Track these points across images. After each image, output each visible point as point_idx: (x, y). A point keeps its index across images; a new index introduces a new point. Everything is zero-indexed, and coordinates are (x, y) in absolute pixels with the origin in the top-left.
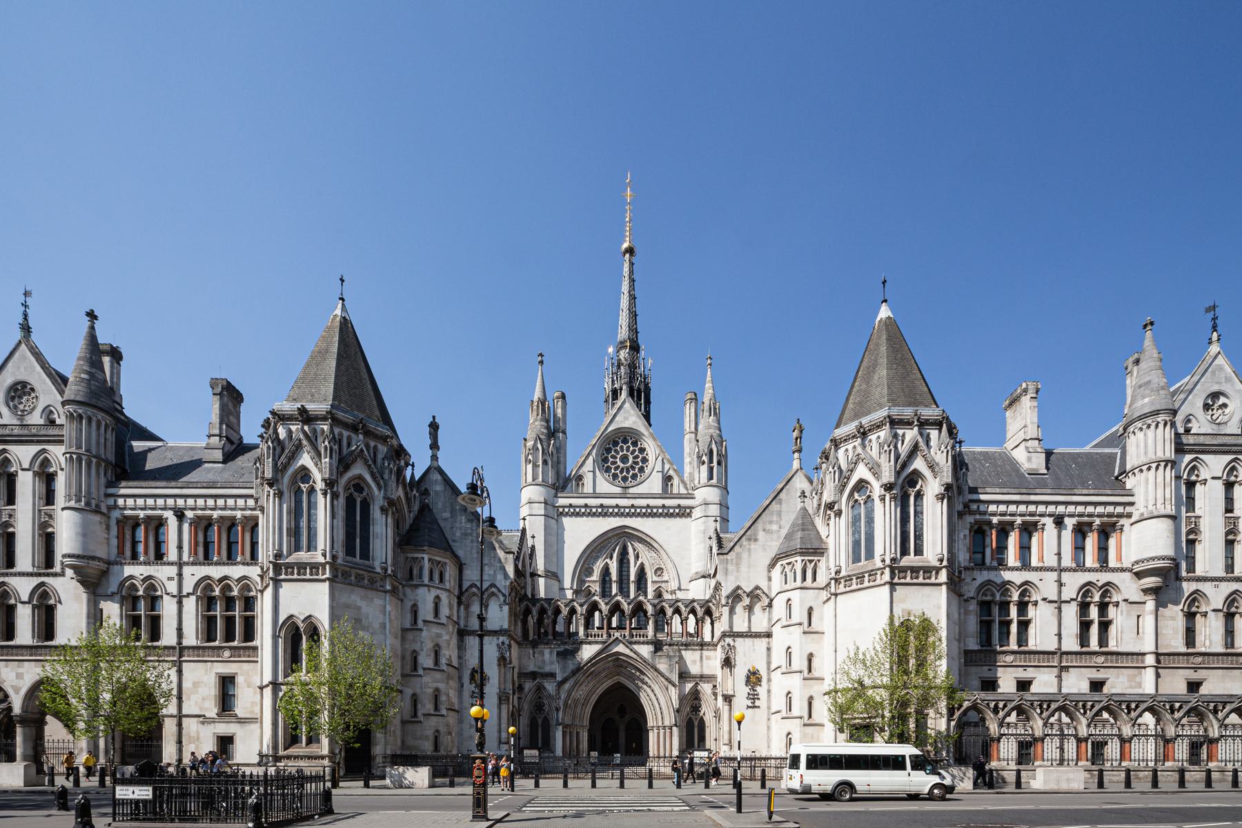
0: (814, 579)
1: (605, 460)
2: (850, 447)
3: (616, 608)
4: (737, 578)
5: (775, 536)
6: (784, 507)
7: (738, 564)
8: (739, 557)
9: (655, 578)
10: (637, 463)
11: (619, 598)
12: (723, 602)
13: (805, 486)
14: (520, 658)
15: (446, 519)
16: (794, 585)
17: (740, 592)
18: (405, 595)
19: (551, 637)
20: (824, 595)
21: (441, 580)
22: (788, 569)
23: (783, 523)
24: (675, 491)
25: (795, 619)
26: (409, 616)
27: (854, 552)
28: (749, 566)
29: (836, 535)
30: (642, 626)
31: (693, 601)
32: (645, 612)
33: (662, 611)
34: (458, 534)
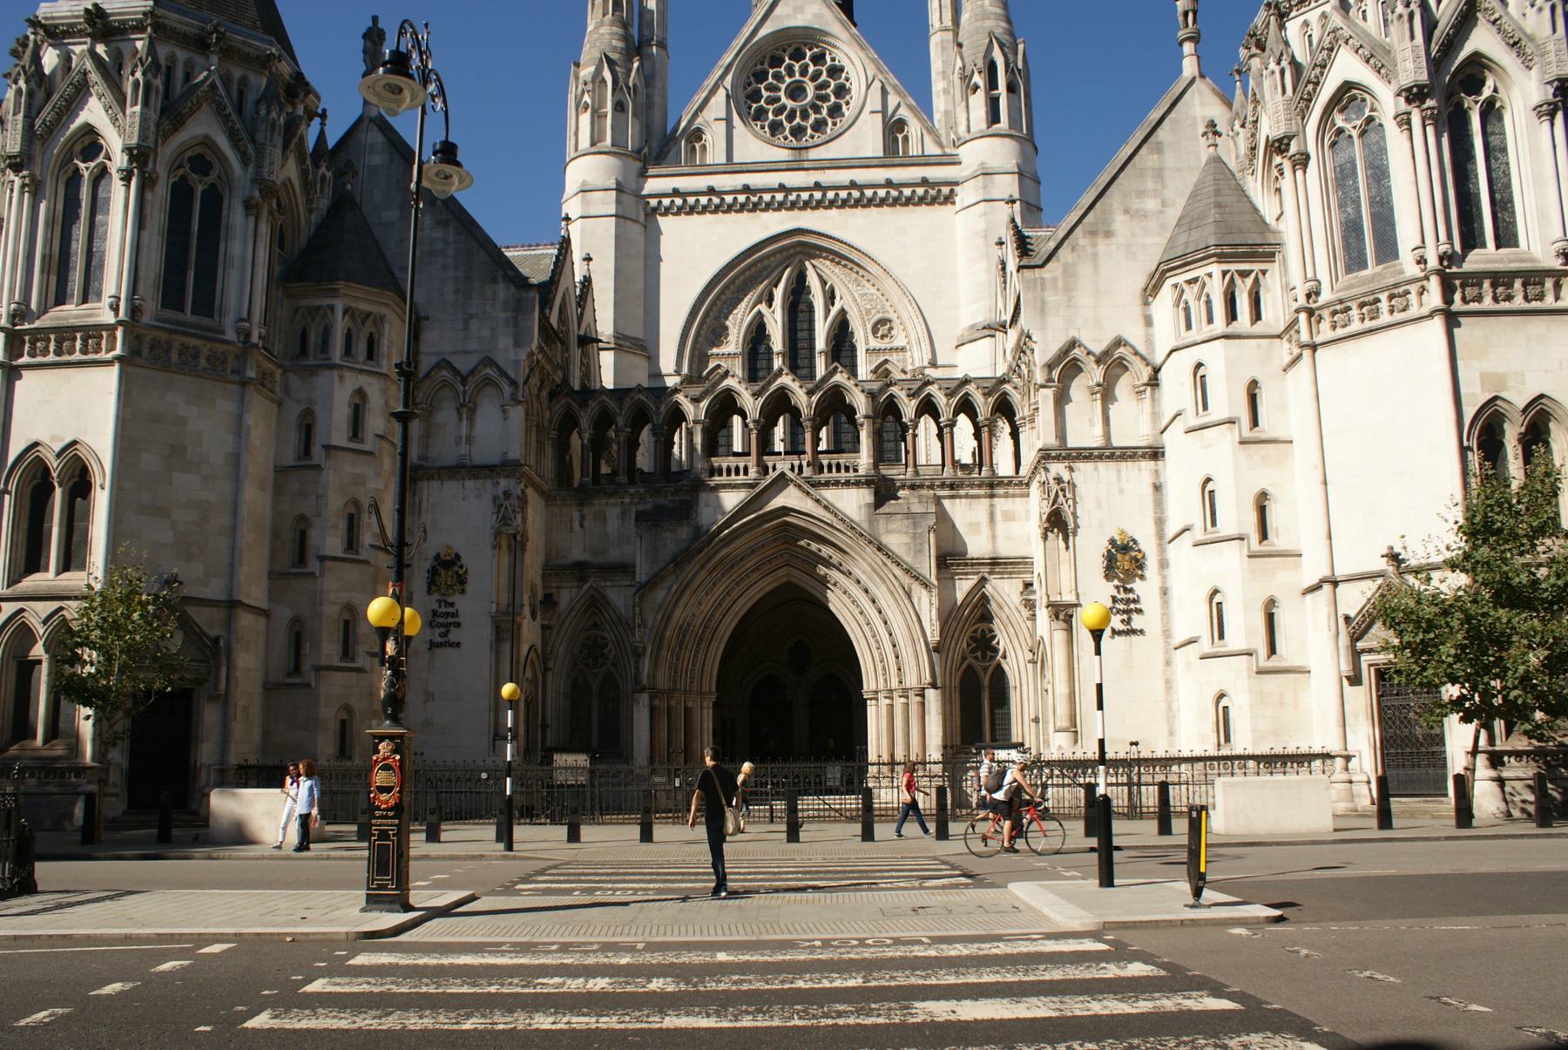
0: (1257, 315)
1: (756, 96)
2: (1313, 16)
3: (779, 404)
6: (1169, 159)
7: (1069, 290)
9: (875, 343)
10: (825, 98)
11: (786, 380)
13: (1217, 111)
14: (548, 532)
16: (1208, 331)
18: (287, 390)
19: (623, 479)
20: (1285, 350)
23: (1169, 194)
25: (1218, 410)
26: (293, 439)
27: (1347, 246)
29: (1299, 212)
30: (844, 443)
31: (966, 381)
32: (851, 411)
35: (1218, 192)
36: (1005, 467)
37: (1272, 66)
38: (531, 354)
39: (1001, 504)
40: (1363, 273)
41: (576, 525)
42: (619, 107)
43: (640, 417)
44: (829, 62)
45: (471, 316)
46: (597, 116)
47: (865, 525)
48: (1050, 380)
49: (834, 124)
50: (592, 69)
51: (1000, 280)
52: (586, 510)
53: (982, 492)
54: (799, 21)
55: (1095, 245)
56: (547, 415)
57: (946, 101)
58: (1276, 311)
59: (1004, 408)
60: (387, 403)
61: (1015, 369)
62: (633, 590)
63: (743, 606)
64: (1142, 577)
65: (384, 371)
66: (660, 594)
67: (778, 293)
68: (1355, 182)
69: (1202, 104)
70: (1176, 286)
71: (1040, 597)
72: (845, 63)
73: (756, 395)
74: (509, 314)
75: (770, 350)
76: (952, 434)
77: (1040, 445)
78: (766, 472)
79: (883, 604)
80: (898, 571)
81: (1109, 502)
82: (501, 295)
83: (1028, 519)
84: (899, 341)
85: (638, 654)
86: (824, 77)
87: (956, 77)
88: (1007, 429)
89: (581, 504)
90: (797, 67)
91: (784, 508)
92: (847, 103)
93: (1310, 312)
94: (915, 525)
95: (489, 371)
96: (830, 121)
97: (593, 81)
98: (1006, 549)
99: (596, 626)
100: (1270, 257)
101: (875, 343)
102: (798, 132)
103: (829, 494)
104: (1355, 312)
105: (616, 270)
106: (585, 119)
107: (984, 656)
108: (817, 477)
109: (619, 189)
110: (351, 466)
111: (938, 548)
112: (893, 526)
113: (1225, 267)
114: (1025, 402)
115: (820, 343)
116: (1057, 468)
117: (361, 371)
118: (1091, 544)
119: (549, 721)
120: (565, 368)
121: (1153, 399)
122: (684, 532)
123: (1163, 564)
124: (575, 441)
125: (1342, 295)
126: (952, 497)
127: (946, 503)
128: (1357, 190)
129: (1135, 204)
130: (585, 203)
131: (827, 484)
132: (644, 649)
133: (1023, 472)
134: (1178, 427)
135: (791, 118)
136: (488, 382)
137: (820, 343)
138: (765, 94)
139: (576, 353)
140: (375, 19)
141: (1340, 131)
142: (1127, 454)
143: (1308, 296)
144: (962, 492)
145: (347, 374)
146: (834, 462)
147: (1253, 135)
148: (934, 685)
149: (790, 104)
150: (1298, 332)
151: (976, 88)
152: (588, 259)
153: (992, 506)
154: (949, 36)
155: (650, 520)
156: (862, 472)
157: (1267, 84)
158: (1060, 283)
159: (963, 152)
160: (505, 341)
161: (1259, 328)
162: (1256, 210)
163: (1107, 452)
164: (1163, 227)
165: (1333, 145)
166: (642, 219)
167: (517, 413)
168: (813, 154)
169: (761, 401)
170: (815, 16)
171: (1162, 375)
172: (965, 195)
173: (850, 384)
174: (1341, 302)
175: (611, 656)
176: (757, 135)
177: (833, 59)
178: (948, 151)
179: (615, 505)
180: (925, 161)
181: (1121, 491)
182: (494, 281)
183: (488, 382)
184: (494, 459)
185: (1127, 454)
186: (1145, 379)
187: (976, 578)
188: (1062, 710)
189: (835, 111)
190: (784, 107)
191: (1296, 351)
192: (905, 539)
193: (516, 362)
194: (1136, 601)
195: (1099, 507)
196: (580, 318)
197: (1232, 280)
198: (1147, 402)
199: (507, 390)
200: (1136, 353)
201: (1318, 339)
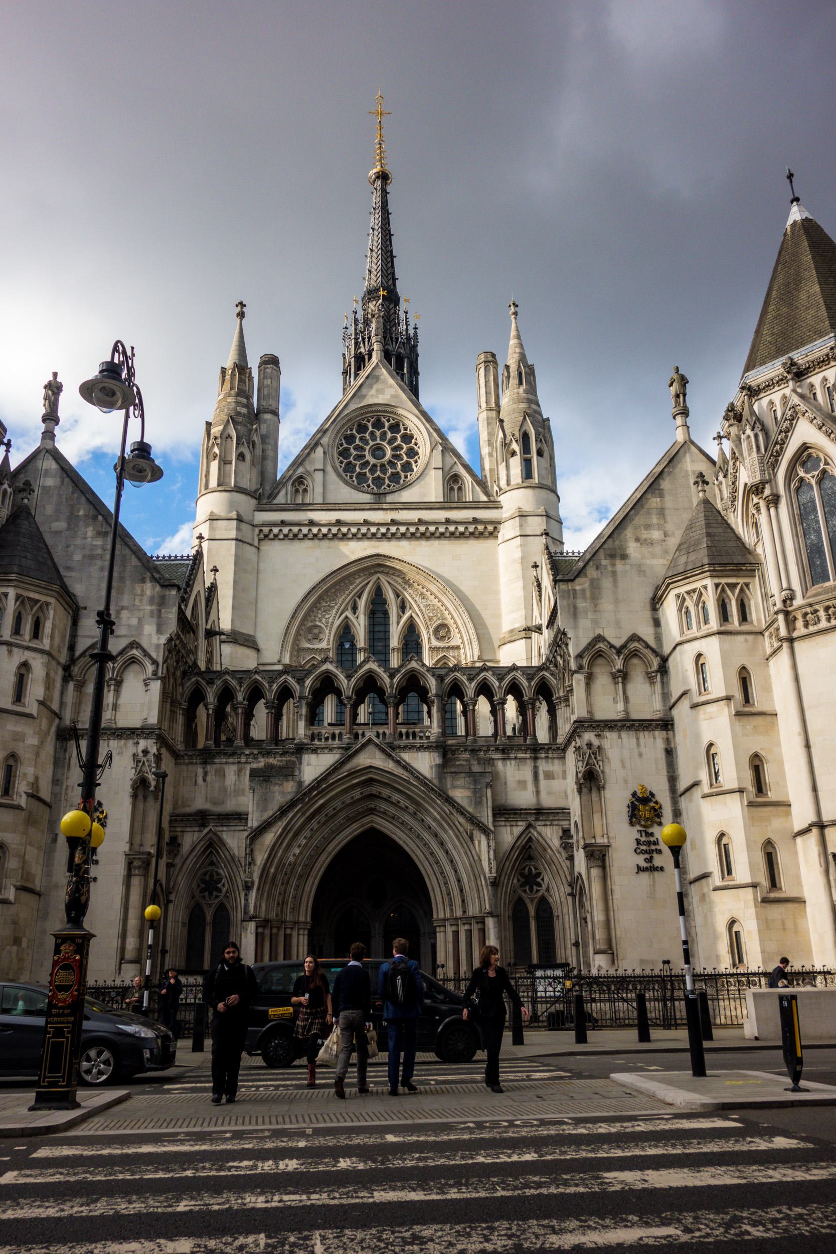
0: (744, 618)
3: (369, 686)
4: (595, 623)
5: (657, 549)
6: (669, 502)
8: (595, 586)
9: (435, 643)
11: (373, 666)
12: (573, 665)
15: (58, 533)
16: (705, 630)
17: (601, 645)
21: (36, 634)
22: (689, 603)
23: (669, 527)
24: (469, 497)
28: (617, 601)
31: (514, 668)
33: (456, 690)
34: (77, 557)
35: (708, 525)
36: (542, 735)
37: (749, 431)
38: (170, 640)
39: (543, 766)
40: (827, 584)
41: (200, 780)
42: (241, 457)
43: (256, 694)
44: (402, 432)
45: (123, 608)
46: (224, 462)
47: (435, 782)
48: (581, 667)
49: (406, 477)
50: (221, 428)
51: (535, 594)
52: (209, 767)
53: (528, 756)
54: (380, 399)
55: (614, 565)
56: (180, 689)
57: (491, 462)
58: (758, 614)
59: (544, 691)
60: (48, 675)
61: (551, 661)
62: (246, 834)
63: (334, 847)
64: (660, 824)
65: (47, 648)
66: (269, 838)
67: (362, 603)
68: (816, 516)
69: (692, 461)
70: (678, 596)
71: (577, 839)
72: (415, 432)
73: (349, 677)
74: (154, 607)
75: (353, 645)
76: (503, 710)
77: (574, 718)
78: (356, 736)
79: (450, 846)
80: (462, 820)
81: (630, 764)
82: (148, 593)
83: (564, 778)
84: (453, 643)
85: (248, 887)
86: (399, 441)
87: (499, 444)
88: (543, 708)
89: (205, 763)
90: (378, 433)
91: (371, 767)
92: (416, 462)
93: (787, 614)
94: (475, 782)
95: (135, 652)
96: (402, 474)
97: (221, 437)
98: (547, 801)
99: (212, 863)
100: (751, 573)
101: (435, 643)
102: (378, 481)
103: (406, 756)
104: (822, 613)
105: (235, 582)
106: (214, 465)
107: (531, 890)
108: (397, 743)
109: (239, 519)
110: (12, 726)
111: (494, 801)
112: (459, 783)
113: (717, 581)
114: (561, 686)
115: (395, 641)
116: (589, 736)
117: (28, 648)
118: (616, 798)
119: (168, 948)
120: (195, 651)
121: (662, 683)
122: (290, 787)
123: (677, 814)
124: (201, 712)
125: (811, 600)
126: (504, 759)
127: (500, 764)
128: (818, 522)
129: (644, 534)
130: (211, 528)
131: (406, 748)
132: (253, 883)
133: (560, 740)
134: (685, 704)
135: (373, 469)
136: (133, 660)
137: (395, 641)
138: (354, 453)
139: (202, 643)
140: (55, 375)
141: (802, 480)
142: (644, 725)
143: (784, 601)
144: (512, 756)
145: (15, 650)
146: (411, 731)
147: (734, 483)
148: (491, 914)
149: (372, 461)
150: (778, 629)
151: (513, 454)
152: (215, 570)
153: (536, 768)
154: (494, 414)
155: (262, 777)
156: (432, 739)
157: (744, 445)
158: (588, 594)
159: (502, 499)
160: (149, 629)
161: (746, 627)
162: (738, 538)
163: (628, 724)
164: (666, 552)
165: (798, 489)
166: (256, 543)
167: (156, 686)
168: (389, 498)
169: (353, 681)
170: (393, 396)
171: (671, 663)
172: (508, 530)
173: (423, 670)
174: (811, 605)
175: (224, 890)
176: (346, 483)
177: (406, 429)
178: (492, 499)
179: (233, 763)
180: (476, 505)
181: (640, 755)
182: (143, 581)
183: (133, 660)
184: (136, 723)
185: (644, 725)
186: (655, 666)
187: (524, 824)
188: (600, 934)
189: (407, 467)
190: (368, 462)
191: (776, 644)
192: (468, 793)
193: (158, 646)
194: (656, 843)
195: (623, 767)
196: (208, 614)
197: (723, 590)
198: (658, 687)
199: (150, 668)
200: (648, 646)
201: (795, 635)
